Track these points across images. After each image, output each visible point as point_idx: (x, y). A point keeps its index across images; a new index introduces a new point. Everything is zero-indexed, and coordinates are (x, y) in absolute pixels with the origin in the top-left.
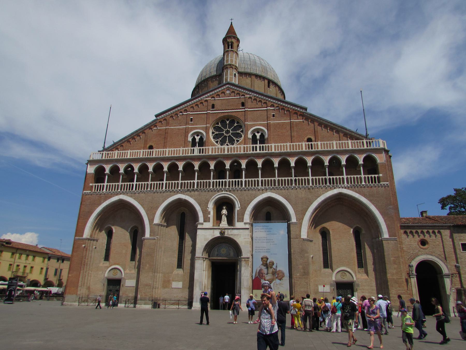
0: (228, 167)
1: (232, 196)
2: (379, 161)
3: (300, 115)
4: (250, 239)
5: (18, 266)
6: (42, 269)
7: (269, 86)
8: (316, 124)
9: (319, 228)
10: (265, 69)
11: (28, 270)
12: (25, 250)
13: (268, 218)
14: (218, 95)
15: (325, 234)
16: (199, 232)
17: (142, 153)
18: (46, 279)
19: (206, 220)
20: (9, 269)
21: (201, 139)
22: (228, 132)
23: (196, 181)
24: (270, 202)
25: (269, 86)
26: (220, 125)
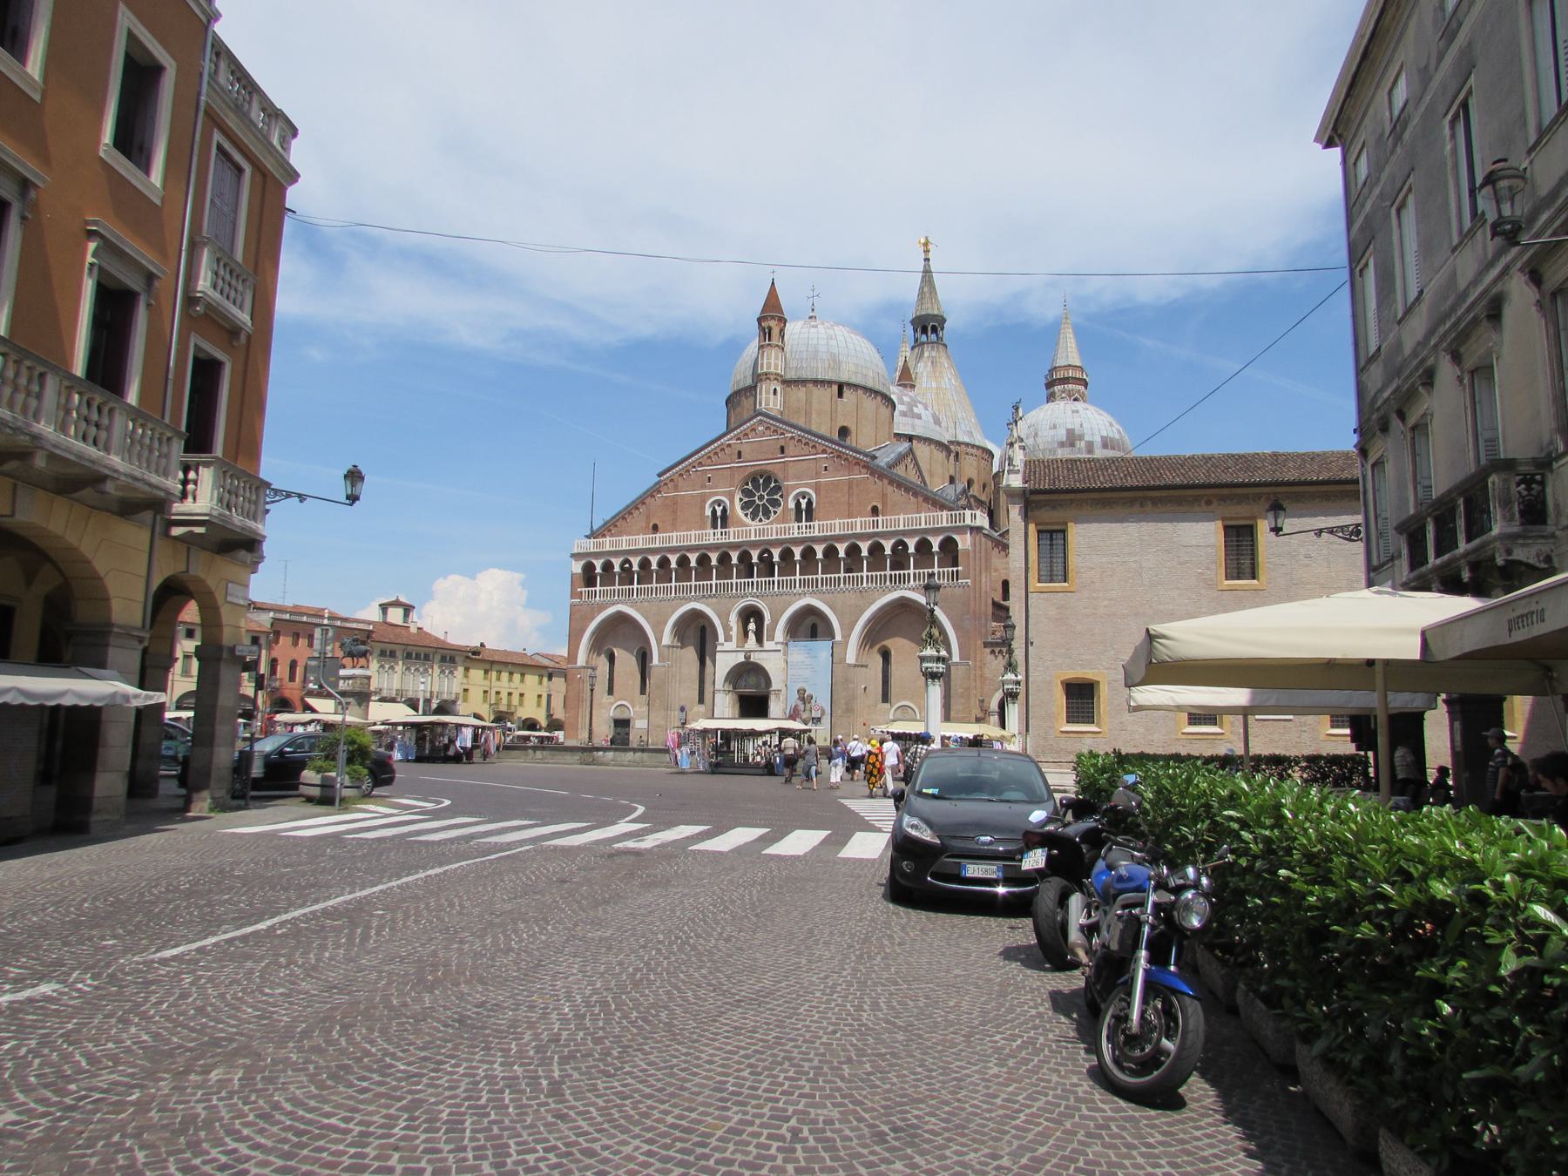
0: (755, 560)
1: (762, 605)
2: (960, 547)
3: (864, 467)
4: (784, 665)
5: (498, 693)
6: (539, 696)
7: (840, 395)
8: (886, 482)
9: (877, 647)
10: (834, 361)
11: (515, 700)
12: (506, 664)
13: (814, 634)
14: (746, 435)
15: (886, 655)
16: (718, 656)
17: (641, 541)
18: (549, 716)
19: (728, 638)
20: (485, 701)
21: (724, 510)
22: (761, 498)
23: (714, 582)
24: (810, 611)
25: (840, 395)
26: (750, 487)
